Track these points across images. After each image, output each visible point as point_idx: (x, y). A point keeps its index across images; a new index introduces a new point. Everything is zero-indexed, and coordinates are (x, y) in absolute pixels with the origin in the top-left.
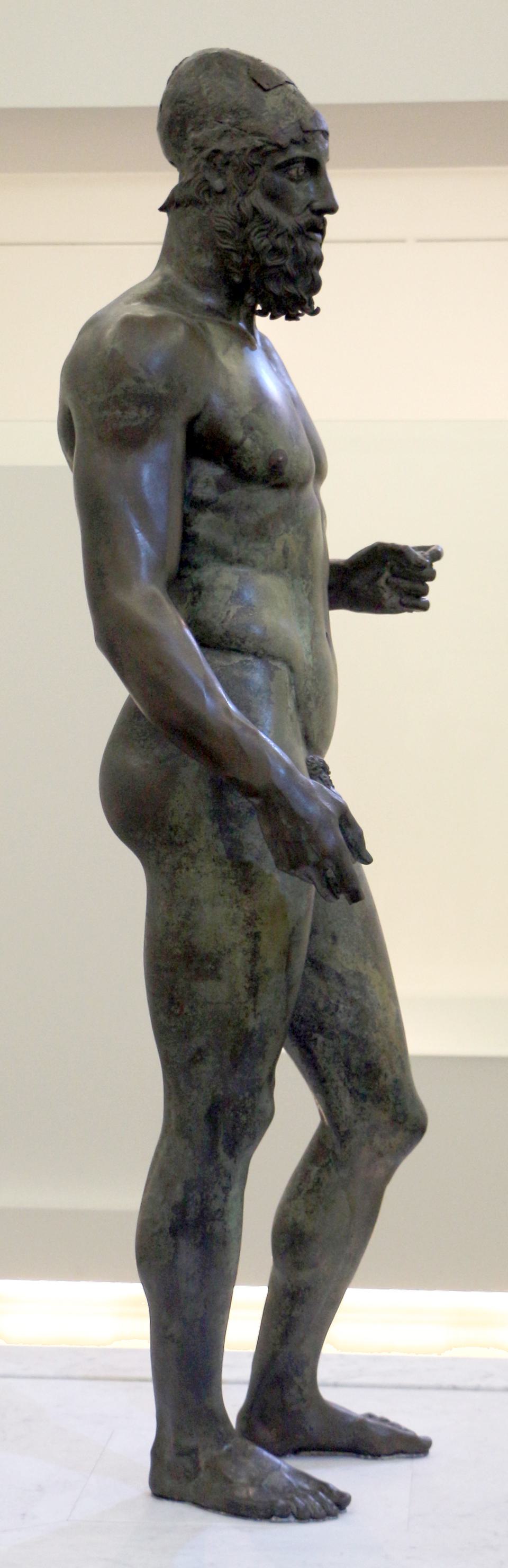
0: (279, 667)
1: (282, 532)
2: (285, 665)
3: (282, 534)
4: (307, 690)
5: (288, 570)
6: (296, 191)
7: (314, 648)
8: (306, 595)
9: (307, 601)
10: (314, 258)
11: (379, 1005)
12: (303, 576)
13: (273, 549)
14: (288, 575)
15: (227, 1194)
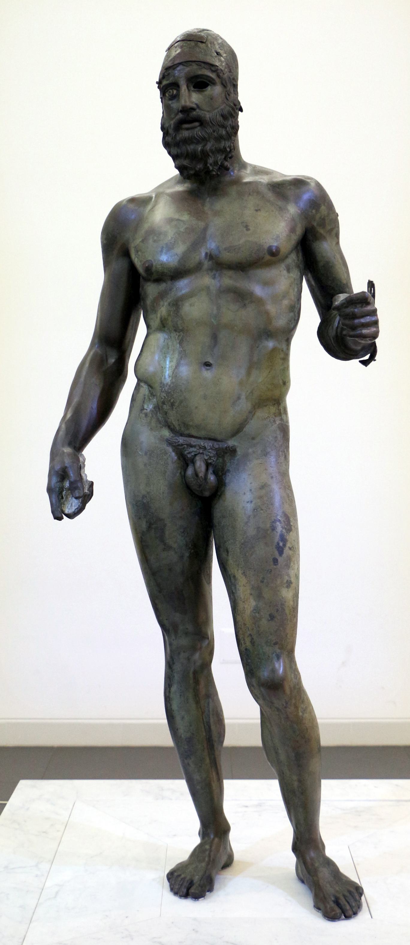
0: (143, 385)
1: (161, 306)
2: (146, 385)
3: (161, 308)
4: (162, 398)
5: (166, 329)
6: (172, 105)
7: (175, 373)
8: (178, 341)
9: (178, 345)
10: (184, 138)
11: (241, 598)
12: (175, 331)
13: (157, 318)
14: (167, 331)
15: (170, 689)
